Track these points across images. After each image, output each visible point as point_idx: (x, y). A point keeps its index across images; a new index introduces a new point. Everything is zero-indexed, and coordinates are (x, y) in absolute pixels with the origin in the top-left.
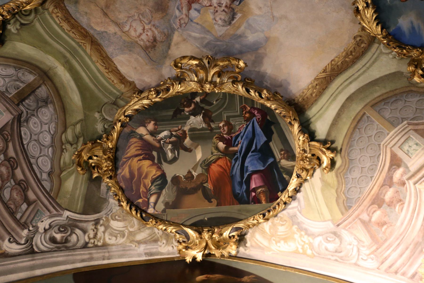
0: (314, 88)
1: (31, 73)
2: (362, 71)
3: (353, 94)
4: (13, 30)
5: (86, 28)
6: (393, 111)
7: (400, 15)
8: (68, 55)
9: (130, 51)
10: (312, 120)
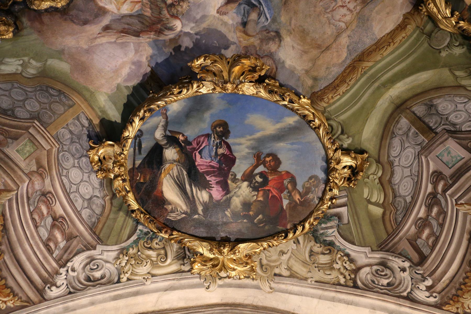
1: (398, 122)
4: (349, 141)
5: (344, 68)
8: (376, 84)
9: (368, 20)
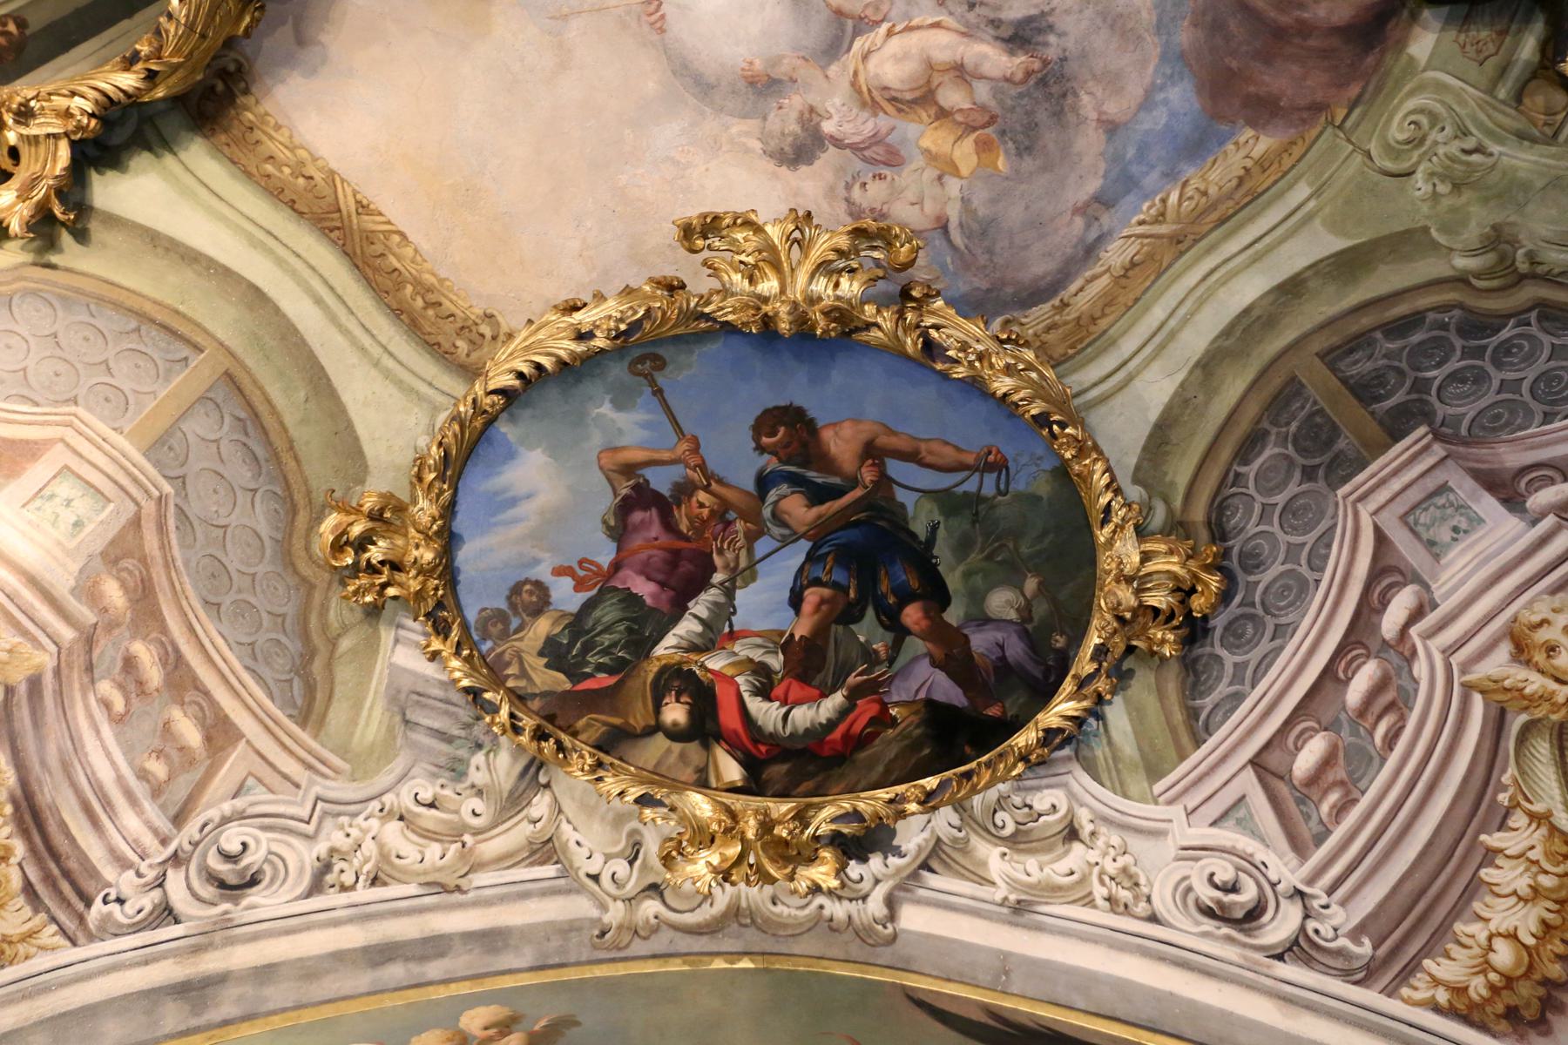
0: (299, 170)
2: (366, 341)
3: (277, 310)
6: (214, 446)
7: (554, 451)
10: (169, 159)
